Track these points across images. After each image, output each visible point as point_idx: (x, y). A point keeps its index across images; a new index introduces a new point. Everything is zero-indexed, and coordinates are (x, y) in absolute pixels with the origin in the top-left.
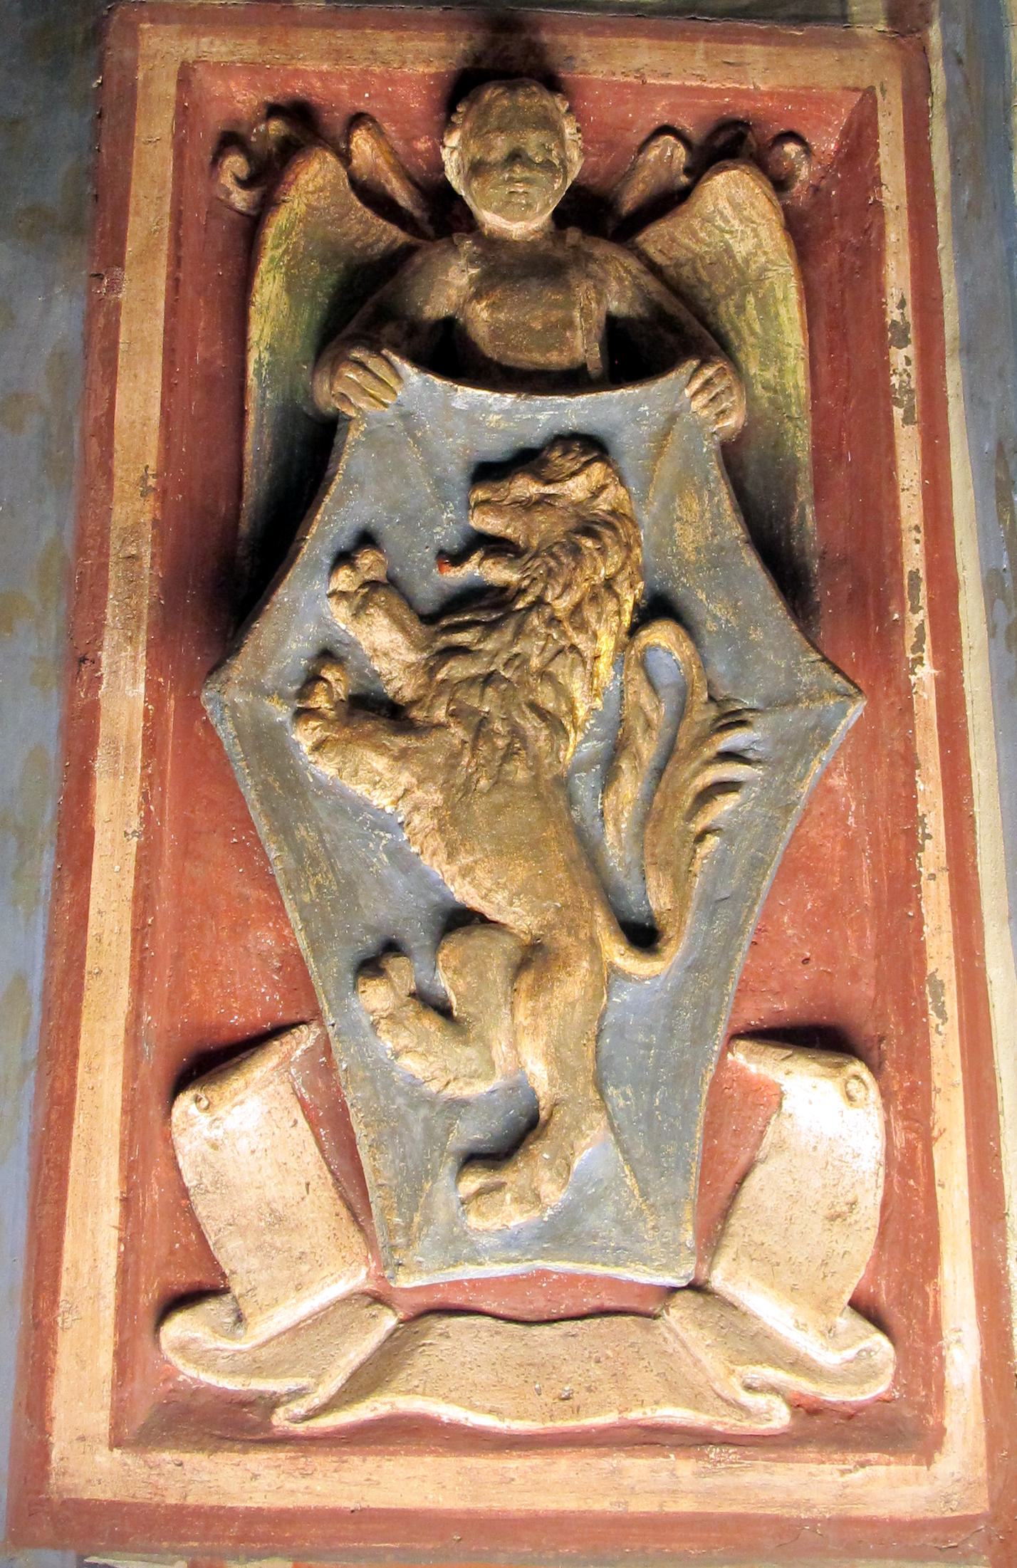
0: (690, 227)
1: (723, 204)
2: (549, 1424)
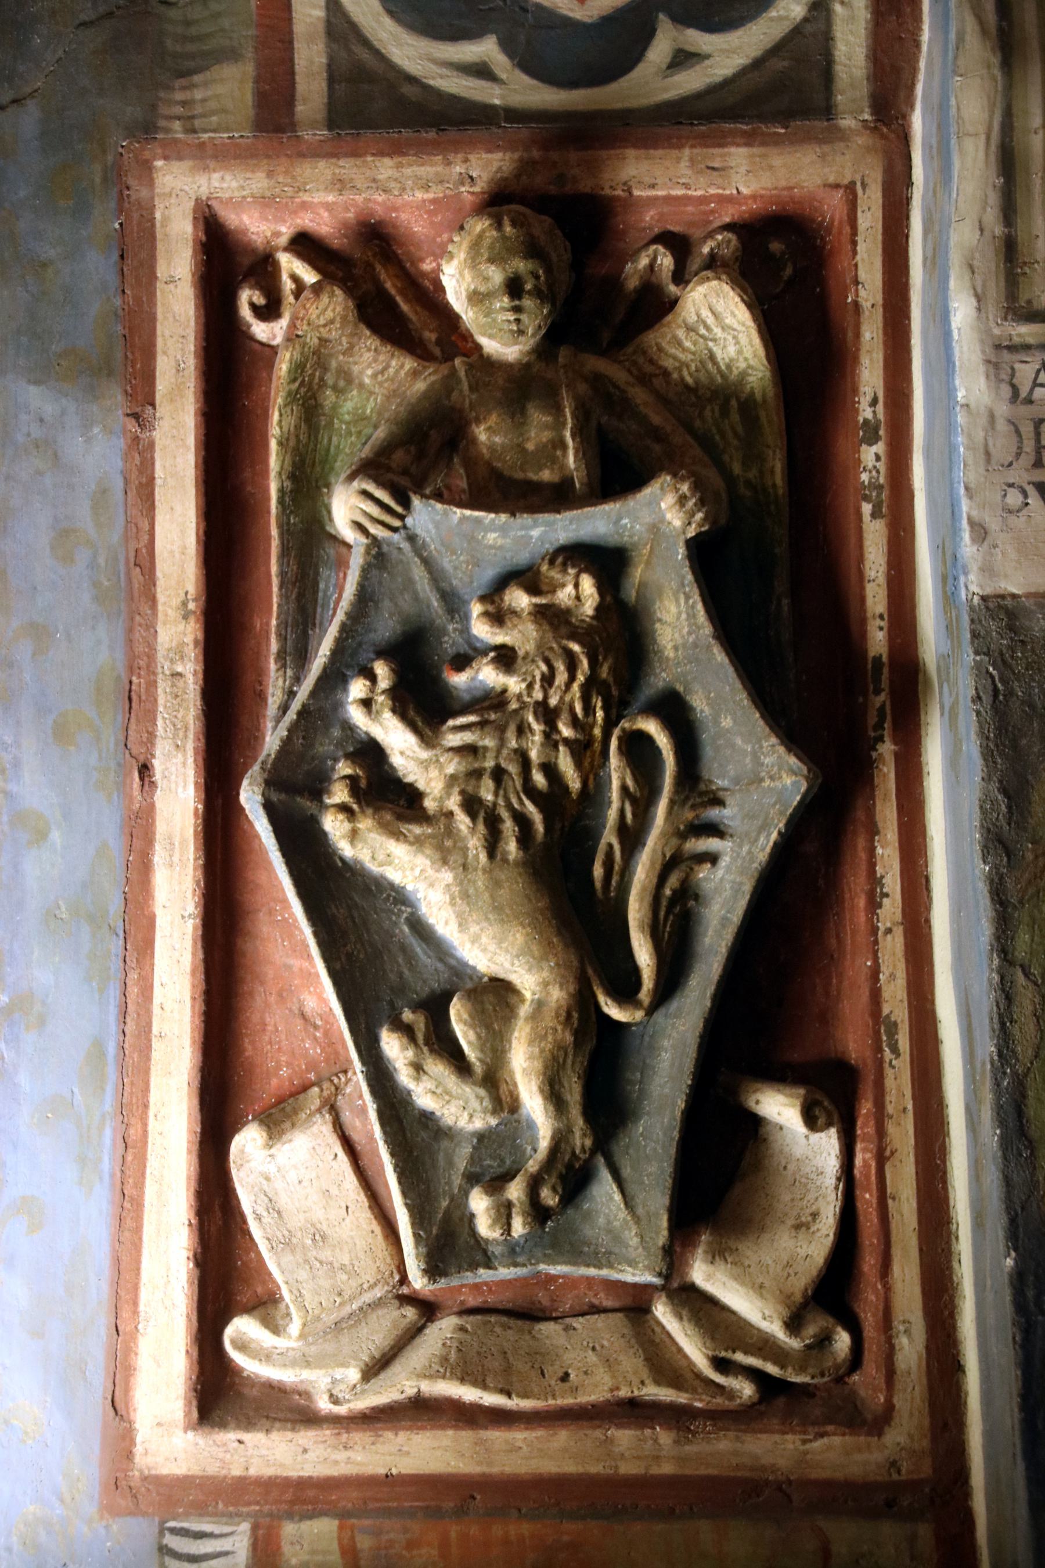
0: (675, 337)
1: (705, 313)
2: (551, 1402)
